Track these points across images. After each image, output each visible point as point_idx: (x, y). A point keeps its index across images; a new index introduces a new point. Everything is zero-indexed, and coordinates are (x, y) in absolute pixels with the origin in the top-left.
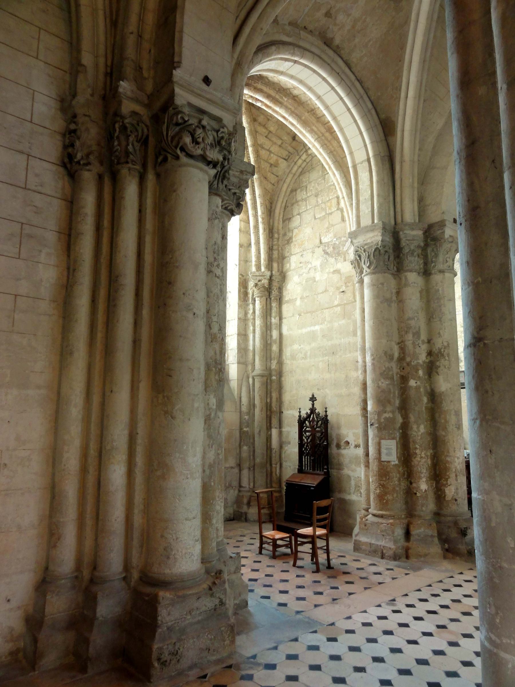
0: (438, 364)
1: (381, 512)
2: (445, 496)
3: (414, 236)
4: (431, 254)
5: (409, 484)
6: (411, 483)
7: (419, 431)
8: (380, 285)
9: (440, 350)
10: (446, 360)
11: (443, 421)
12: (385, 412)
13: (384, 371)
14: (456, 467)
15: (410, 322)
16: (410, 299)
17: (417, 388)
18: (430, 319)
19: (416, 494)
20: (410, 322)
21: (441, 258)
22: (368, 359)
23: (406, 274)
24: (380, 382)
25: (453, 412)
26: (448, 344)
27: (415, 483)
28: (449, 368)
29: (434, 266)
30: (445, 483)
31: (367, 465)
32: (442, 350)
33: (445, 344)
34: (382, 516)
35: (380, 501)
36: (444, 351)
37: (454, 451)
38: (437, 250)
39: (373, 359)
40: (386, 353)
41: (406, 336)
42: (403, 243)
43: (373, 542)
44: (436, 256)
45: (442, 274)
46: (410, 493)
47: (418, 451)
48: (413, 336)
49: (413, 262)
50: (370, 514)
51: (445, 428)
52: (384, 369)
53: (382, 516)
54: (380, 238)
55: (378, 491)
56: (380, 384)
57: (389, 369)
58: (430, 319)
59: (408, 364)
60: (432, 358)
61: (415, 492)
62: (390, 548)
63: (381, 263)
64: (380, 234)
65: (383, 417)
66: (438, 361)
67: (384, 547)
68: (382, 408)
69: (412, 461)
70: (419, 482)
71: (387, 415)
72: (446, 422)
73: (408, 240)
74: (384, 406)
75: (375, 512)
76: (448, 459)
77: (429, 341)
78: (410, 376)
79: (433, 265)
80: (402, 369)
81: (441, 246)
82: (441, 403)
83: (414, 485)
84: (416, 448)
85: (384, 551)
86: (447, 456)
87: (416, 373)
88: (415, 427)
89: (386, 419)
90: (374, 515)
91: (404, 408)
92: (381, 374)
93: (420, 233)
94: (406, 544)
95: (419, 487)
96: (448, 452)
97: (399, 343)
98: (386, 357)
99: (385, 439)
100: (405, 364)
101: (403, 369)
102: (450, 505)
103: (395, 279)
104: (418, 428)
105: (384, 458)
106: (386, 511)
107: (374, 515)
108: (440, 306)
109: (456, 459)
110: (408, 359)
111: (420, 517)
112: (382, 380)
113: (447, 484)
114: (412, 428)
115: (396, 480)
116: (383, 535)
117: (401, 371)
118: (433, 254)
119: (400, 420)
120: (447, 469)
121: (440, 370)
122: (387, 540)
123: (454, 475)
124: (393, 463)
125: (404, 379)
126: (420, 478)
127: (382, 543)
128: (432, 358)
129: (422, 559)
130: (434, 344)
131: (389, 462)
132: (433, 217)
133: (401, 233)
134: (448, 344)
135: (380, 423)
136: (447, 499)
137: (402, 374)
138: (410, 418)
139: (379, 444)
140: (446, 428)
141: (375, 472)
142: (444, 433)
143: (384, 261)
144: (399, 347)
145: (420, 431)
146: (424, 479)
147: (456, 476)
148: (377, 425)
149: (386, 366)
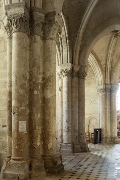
0: (47, 84)
1: (17, 158)
2: (48, 147)
3: (40, 16)
4: (47, 29)
5: (31, 143)
6: (32, 143)
7: (38, 117)
8: (22, 39)
9: (49, 77)
10: (51, 82)
11: (48, 112)
12: (22, 107)
13: (22, 85)
14: (53, 134)
15: (36, 61)
16: (37, 49)
17: (38, 95)
18: (44, 62)
19: (35, 147)
20: (36, 61)
21: (51, 33)
22: (13, 78)
23: (35, 36)
24: (19, 91)
25: (53, 108)
26: (53, 75)
27: (35, 142)
28: (52, 87)
29: (48, 36)
30: (48, 141)
31: (10, 135)
32: (50, 78)
33: (51, 75)
34: (18, 160)
35: (17, 152)
36: (51, 78)
37: (53, 126)
38: (50, 27)
39: (16, 78)
40: (23, 76)
41: (33, 68)
42: (35, 18)
43: (13, 173)
44: (50, 30)
45: (51, 40)
46: (32, 147)
47: (37, 127)
48: (37, 69)
49: (39, 30)
50: (11, 159)
51: (49, 116)
52: (22, 84)
53: (18, 160)
54: (23, 12)
55: (16, 147)
56: (20, 92)
57: (24, 84)
58: (44, 62)
59: (34, 83)
60: (45, 81)
61: (35, 146)
62: (23, 175)
63: (23, 27)
64: (23, 9)
65: (21, 109)
66: (47, 83)
67: (19, 175)
68: (20, 104)
69: (34, 131)
70: (36, 141)
71: (22, 108)
72: (50, 112)
73: (38, 18)
74: (21, 103)
75: (14, 158)
76: (50, 130)
77: (43, 73)
78: (34, 89)
79: (47, 35)
80: (30, 85)
81: (52, 25)
82: (48, 103)
83: (34, 143)
84: (36, 125)
85: (20, 177)
86: (49, 129)
87: (38, 87)
88: (36, 114)
89: (22, 110)
90: (14, 160)
91: (31, 105)
92: (20, 86)
93: (43, 15)
94: (30, 172)
95: (37, 144)
96: (50, 127)
97: (29, 72)
98: (23, 78)
99: (21, 120)
100: (32, 83)
101: (31, 85)
102: (50, 152)
103: (29, 38)
104: (37, 115)
105: (20, 130)
106: (20, 157)
107: (14, 160)
108: (50, 56)
109: (53, 130)
110: (34, 80)
111: (36, 158)
112: (21, 90)
113: (49, 142)
114: (34, 115)
115: (26, 142)
116: (19, 169)
117: (30, 87)
118: (48, 29)
119: (28, 111)
120: (49, 135)
121: (48, 87)
122: (21, 171)
123: (52, 137)
124: (24, 133)
125: (31, 91)
126: (37, 140)
127: (18, 173)
128: (45, 81)
129: (37, 178)
130: (46, 74)
131: (23, 132)
132: (50, 10)
133: (34, 12)
134: (53, 75)
135: (18, 112)
136: (48, 149)
137: (30, 88)
138: (33, 110)
139: (18, 123)
140: (50, 116)
141: (15, 138)
142: (48, 118)
143: (24, 27)
144: (30, 74)
145: (38, 116)
146: (39, 140)
147: (53, 138)
148: (17, 113)
149: (23, 83)
